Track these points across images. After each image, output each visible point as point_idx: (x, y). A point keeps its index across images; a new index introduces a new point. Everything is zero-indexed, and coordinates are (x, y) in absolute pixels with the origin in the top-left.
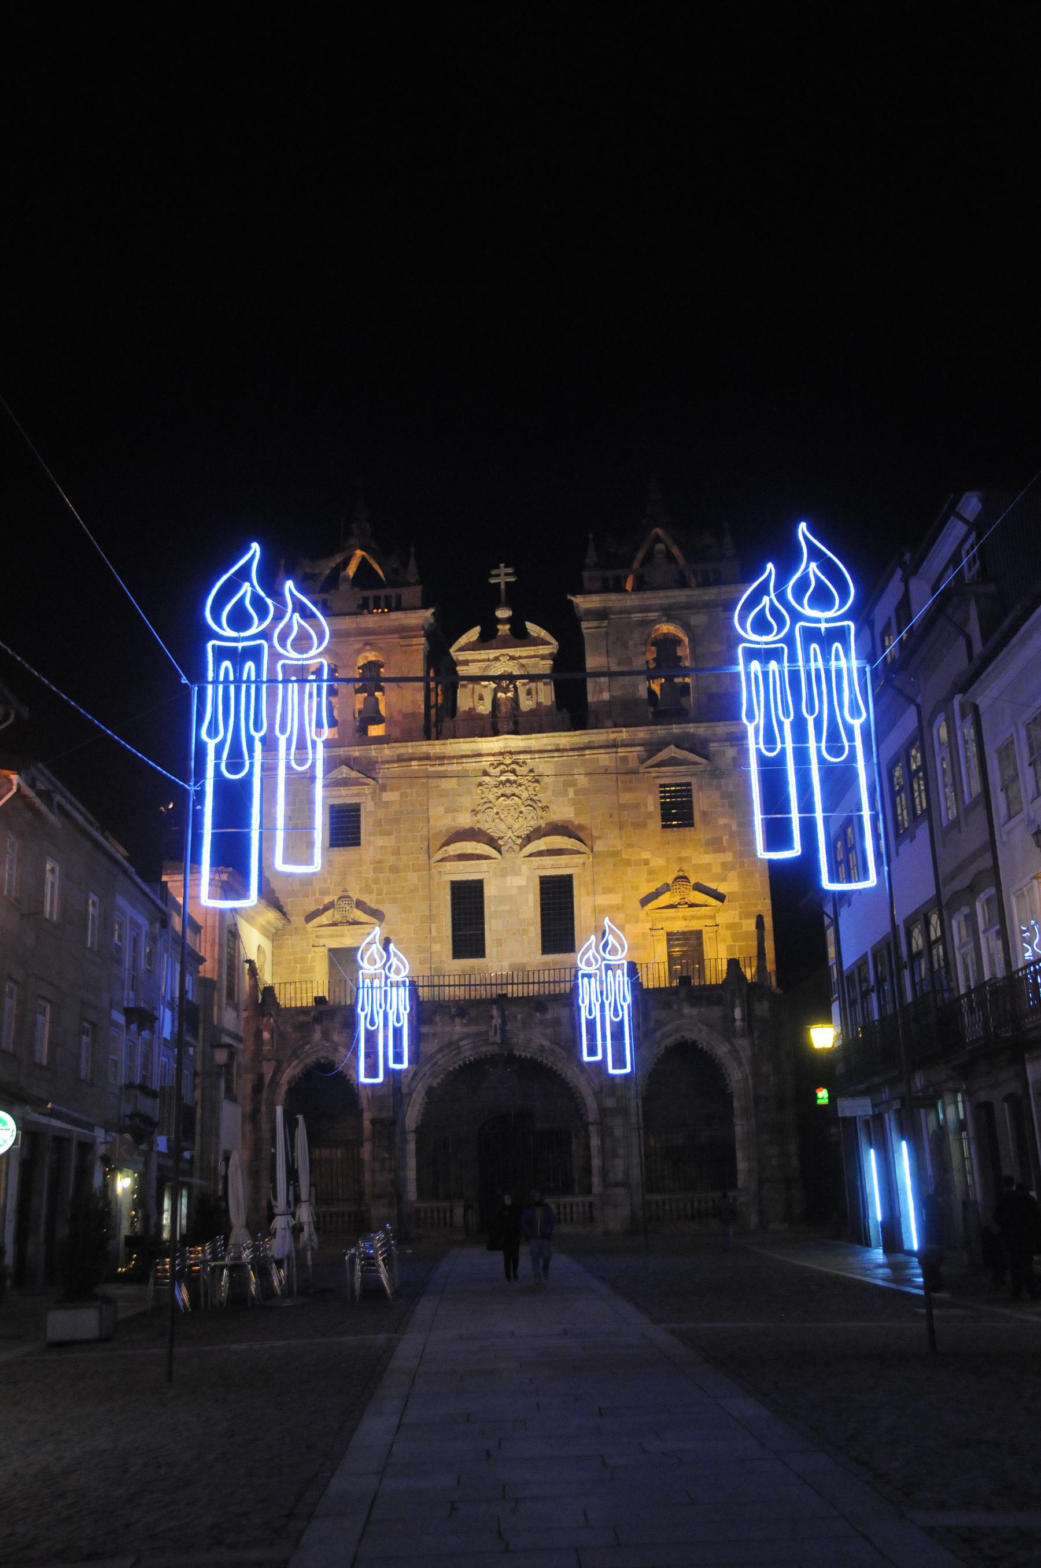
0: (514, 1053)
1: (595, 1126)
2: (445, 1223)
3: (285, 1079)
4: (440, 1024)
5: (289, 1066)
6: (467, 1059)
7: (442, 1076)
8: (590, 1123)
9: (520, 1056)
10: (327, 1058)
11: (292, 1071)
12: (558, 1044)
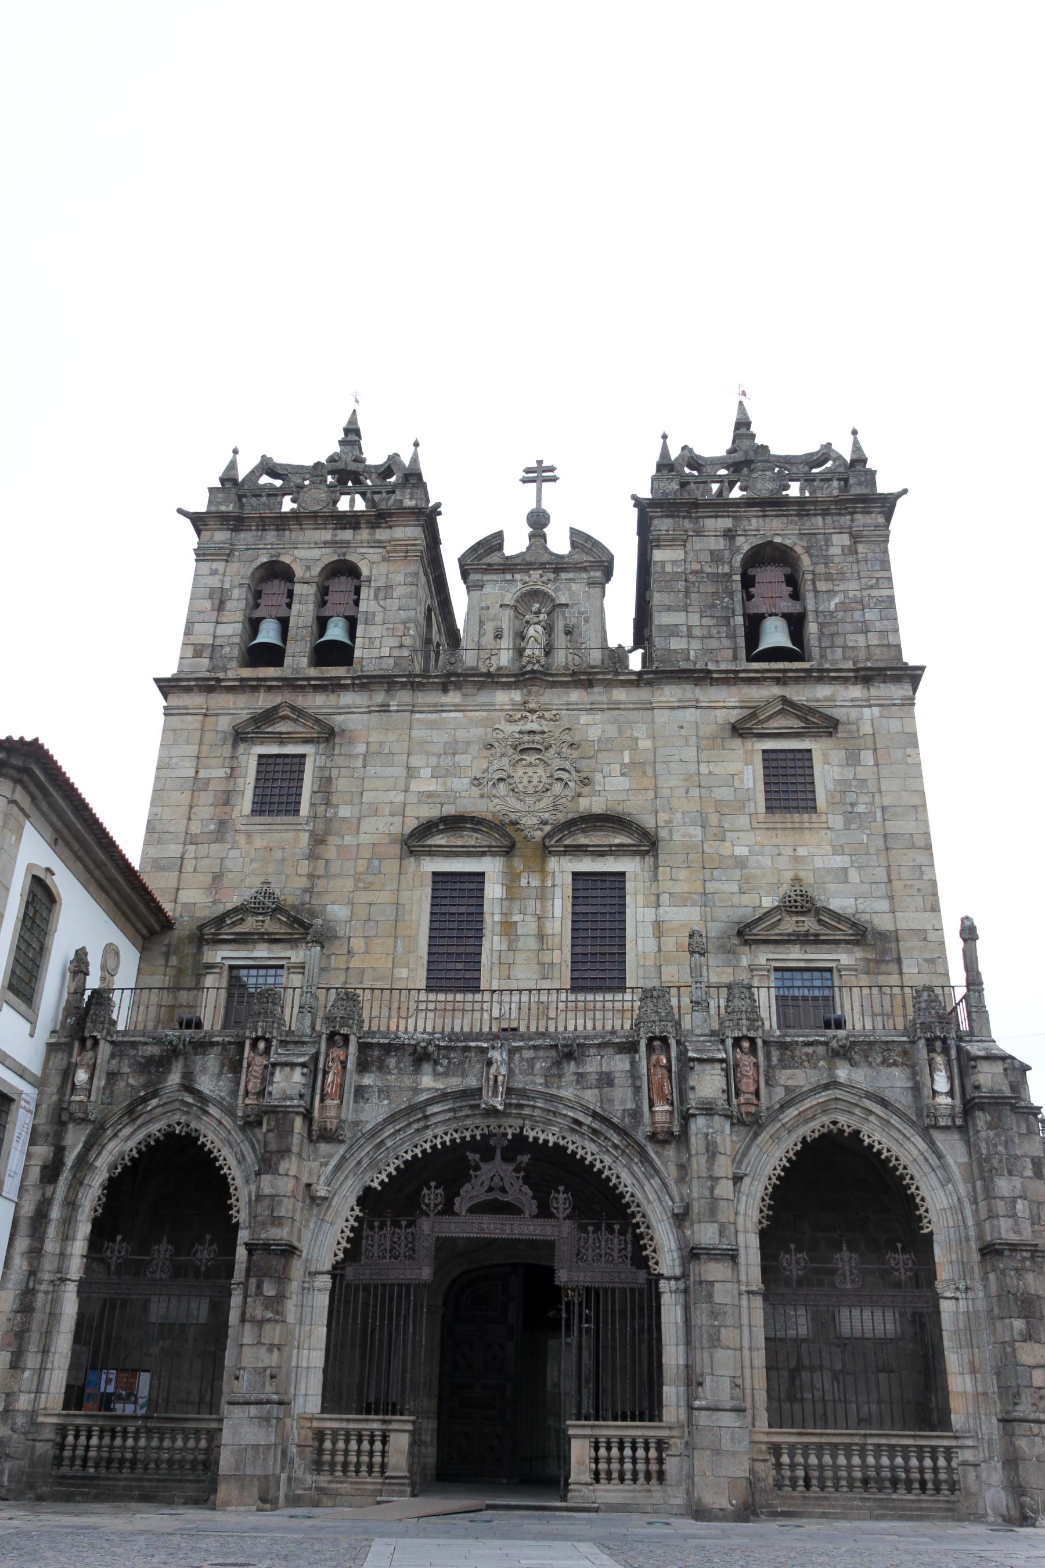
2: (370, 1466)
4: (396, 1071)
5: (116, 1135)
6: (438, 1141)
7: (391, 1169)
8: (661, 1276)
9: (536, 1139)
10: (188, 1126)
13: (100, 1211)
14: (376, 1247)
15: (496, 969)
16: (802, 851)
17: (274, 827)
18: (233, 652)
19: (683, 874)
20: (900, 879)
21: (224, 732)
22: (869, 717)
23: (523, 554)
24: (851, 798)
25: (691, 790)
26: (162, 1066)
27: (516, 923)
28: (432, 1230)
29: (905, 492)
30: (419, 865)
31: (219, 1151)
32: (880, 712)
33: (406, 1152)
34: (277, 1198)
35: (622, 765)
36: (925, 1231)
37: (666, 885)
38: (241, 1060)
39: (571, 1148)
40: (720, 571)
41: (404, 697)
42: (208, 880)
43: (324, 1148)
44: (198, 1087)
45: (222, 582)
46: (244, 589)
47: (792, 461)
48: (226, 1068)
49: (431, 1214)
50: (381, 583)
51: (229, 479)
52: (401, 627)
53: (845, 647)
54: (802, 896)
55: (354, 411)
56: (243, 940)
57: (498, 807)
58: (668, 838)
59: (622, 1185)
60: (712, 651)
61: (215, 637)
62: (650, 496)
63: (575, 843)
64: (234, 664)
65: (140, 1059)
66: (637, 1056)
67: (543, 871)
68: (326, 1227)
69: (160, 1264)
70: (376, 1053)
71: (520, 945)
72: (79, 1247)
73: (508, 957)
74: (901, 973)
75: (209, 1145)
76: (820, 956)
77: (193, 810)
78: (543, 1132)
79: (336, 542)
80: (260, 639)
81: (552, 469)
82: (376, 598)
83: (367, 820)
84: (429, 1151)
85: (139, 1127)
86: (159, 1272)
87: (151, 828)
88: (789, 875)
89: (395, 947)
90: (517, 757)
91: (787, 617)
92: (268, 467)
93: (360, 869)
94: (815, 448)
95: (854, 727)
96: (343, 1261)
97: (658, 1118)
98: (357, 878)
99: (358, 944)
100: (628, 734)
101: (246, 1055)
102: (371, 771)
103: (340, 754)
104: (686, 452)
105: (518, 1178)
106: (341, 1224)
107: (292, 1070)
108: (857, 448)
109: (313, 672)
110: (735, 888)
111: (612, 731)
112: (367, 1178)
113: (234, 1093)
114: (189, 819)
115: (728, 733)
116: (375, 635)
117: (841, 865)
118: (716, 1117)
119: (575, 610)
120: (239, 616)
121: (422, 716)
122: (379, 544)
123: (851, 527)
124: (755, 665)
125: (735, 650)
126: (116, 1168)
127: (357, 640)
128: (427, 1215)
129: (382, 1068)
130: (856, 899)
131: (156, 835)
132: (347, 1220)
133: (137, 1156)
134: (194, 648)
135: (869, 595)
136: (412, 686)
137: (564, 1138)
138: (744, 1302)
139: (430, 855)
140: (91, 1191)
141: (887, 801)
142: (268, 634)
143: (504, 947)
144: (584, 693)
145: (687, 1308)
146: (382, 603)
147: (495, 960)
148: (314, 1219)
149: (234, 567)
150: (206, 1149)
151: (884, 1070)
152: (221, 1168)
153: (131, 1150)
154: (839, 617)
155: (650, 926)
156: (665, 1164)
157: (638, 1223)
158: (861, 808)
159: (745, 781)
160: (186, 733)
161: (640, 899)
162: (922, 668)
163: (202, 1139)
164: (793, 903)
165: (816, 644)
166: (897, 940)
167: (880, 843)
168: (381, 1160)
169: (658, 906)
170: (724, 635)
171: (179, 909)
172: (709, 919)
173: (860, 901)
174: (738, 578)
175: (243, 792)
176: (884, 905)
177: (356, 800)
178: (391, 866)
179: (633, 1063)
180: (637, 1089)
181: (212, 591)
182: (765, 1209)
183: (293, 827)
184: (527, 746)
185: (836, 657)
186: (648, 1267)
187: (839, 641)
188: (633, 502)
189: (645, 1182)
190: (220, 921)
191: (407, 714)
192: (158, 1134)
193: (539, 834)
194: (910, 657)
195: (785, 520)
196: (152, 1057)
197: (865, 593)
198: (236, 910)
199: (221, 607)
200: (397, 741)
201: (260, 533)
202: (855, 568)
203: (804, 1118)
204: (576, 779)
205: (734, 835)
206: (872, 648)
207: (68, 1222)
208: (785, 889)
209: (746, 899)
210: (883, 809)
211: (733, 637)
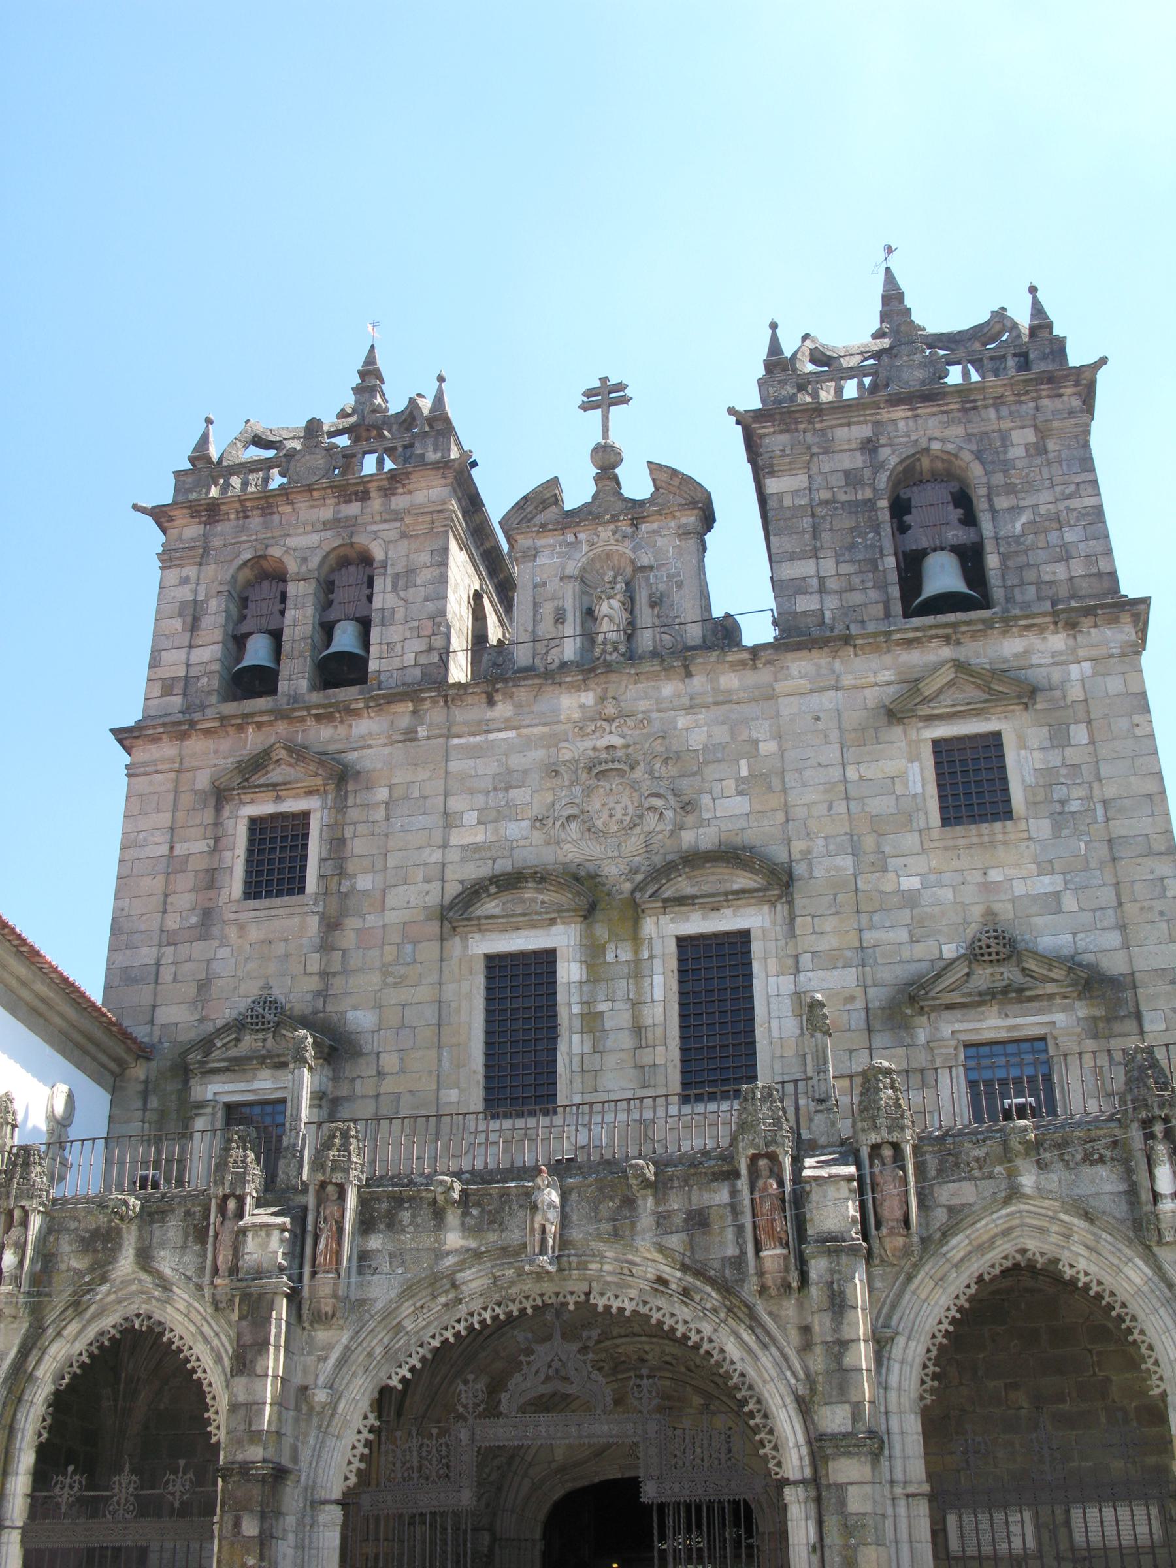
0: (592, 1301)
1: (800, 1490)
4: (411, 1229)
5: (59, 1334)
6: (476, 1319)
7: (415, 1361)
8: (786, 1482)
9: (608, 1308)
10: (150, 1318)
12: (699, 1274)
13: (45, 1435)
14: (399, 1465)
15: (578, 1081)
16: (995, 875)
17: (273, 912)
18: (210, 683)
19: (829, 924)
20: (1135, 901)
21: (204, 792)
22: (1079, 677)
23: (586, 505)
24: (1060, 792)
25: (835, 804)
26: (110, 1241)
27: (602, 1013)
28: (473, 1440)
29: (1103, 361)
30: (466, 947)
31: (191, 1348)
32: (1093, 668)
33: (433, 1337)
34: (255, 1407)
35: (740, 780)
36: (1156, 1392)
37: (807, 941)
38: (208, 1225)
39: (656, 1316)
40: (860, 497)
42: (192, 990)
43: (322, 1335)
44: (155, 1265)
45: (195, 592)
46: (223, 599)
47: (958, 338)
48: (191, 1238)
49: (471, 1419)
50: (399, 569)
51: (200, 455)
52: (429, 623)
53: (1039, 583)
54: (996, 938)
55: (372, 347)
56: (236, 1067)
57: (570, 855)
58: (806, 875)
59: (728, 1361)
60: (854, 608)
61: (188, 666)
62: (758, 405)
63: (677, 895)
64: (213, 699)
65: (82, 1233)
66: (739, 1183)
67: (636, 939)
68: (331, 1442)
69: (123, 1501)
70: (384, 1206)
71: (609, 1044)
73: (593, 1062)
74: (1142, 1032)
75: (177, 1343)
77: (169, 900)
78: (617, 1297)
79: (339, 520)
80: (246, 663)
81: (620, 387)
82: (395, 588)
83: (394, 891)
84: (464, 1333)
85: (89, 1321)
86: (121, 1512)
88: (977, 911)
89: (439, 1061)
90: (593, 782)
91: (957, 550)
93: (388, 958)
94: (984, 317)
95: (1058, 693)
96: (357, 1485)
97: (769, 1265)
98: (385, 971)
99: (390, 1061)
100: (745, 736)
101: (212, 1221)
102: (397, 824)
103: (355, 805)
104: (808, 343)
105: (585, 1362)
106: (350, 1437)
107: (268, 1235)
108: (1038, 310)
109: (316, 697)
110: (903, 936)
111: (721, 734)
112: (383, 1375)
113: (201, 1270)
114: (165, 912)
115: (884, 720)
116: (396, 638)
117: (1050, 889)
118: (844, 1259)
119: (663, 572)
120: (218, 635)
121: (462, 741)
122: (397, 516)
123: (1034, 417)
124: (916, 621)
125: (887, 605)
126: (63, 1378)
127: (372, 649)
128: (465, 1419)
129: (392, 1225)
130: (1074, 934)
131: (124, 937)
132: (359, 1432)
133: (87, 1361)
135: (1067, 508)
136: (446, 702)
137: (645, 1303)
138: (902, 1510)
139: (480, 931)
140: (32, 1410)
141: (1110, 791)
142: (257, 652)
143: (587, 1048)
144: (681, 686)
145: (820, 1523)
146: (402, 594)
147: (576, 1068)
148: (314, 1432)
149: (210, 570)
150: (174, 1347)
151: (1087, 1171)
152: (194, 1371)
153: (81, 1354)
154: (1029, 542)
155: (788, 1001)
156: (783, 1329)
157: (751, 1412)
158: (1074, 806)
159: (911, 784)
160: (156, 797)
161: (772, 964)
162: (1146, 601)
163: (168, 1335)
164: (985, 950)
165: (999, 583)
166: (1135, 987)
167: (1103, 851)
168: (400, 1349)
169: (798, 971)
170: (870, 584)
171: (157, 1033)
172: (869, 982)
173: (1080, 936)
174: (884, 503)
175: (231, 869)
176: (1113, 939)
177: (379, 865)
178: (430, 950)
179: (734, 1193)
180: (740, 1229)
181: (183, 605)
182: (927, 1379)
183: (297, 910)
184: (604, 767)
185: (1027, 598)
186: (769, 1470)
187: (1030, 575)
188: (733, 419)
189: (759, 1352)
190: (206, 1044)
191: (441, 740)
192: (113, 1331)
193: (628, 886)
194: (1130, 588)
195: (945, 418)
196: (97, 1229)
197: (1062, 506)
198: (227, 1028)
199: (194, 626)
200: (430, 779)
201: (241, 522)
202: (1045, 470)
203: (981, 1248)
204: (677, 806)
205: (900, 861)
206: (1077, 580)
208: (972, 930)
209: (923, 950)
210: (1105, 803)
211: (882, 586)
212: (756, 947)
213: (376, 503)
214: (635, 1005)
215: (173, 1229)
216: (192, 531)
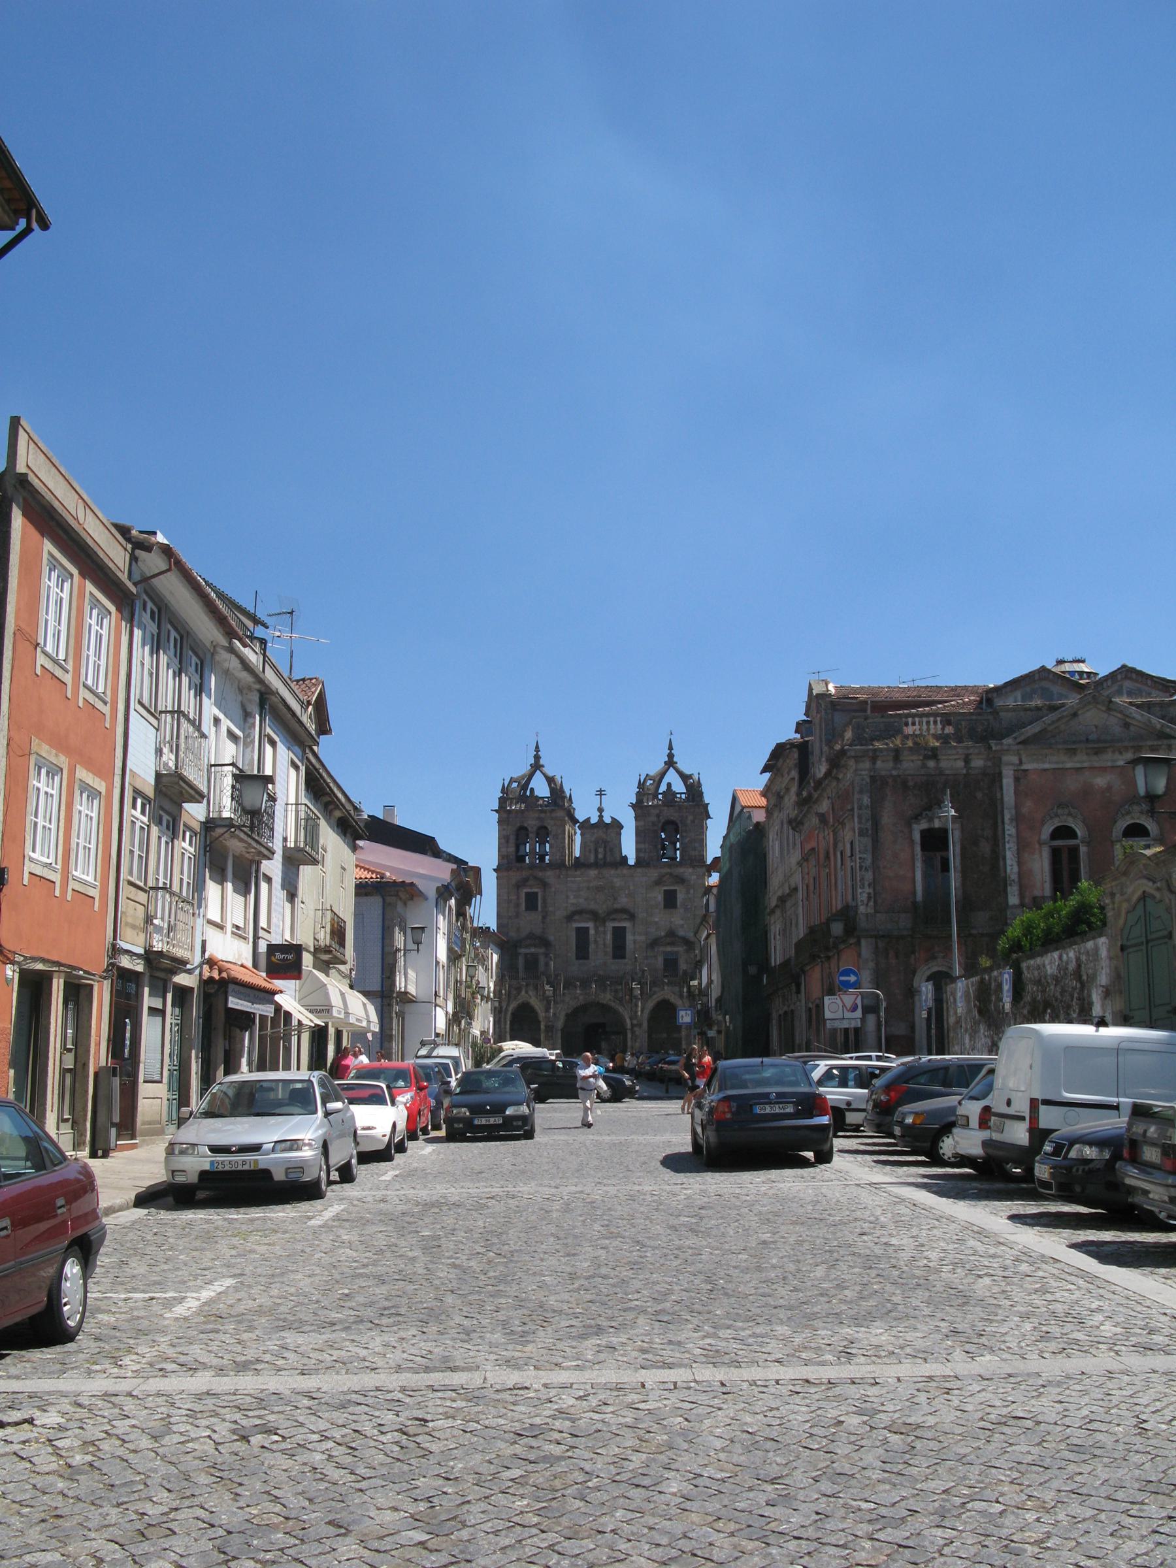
3: (510, 1009)
11: (513, 1005)
18: (513, 857)
41: (564, 872)
56: (527, 946)
67: (605, 926)
72: (508, 1026)
76: (676, 949)
87: (499, 916)
92: (512, 780)
122: (552, 819)
134: (501, 856)
207: (505, 1023)
212: (627, 930)
213: (548, 814)
214: (604, 939)
215: (531, 988)
216: (505, 815)
